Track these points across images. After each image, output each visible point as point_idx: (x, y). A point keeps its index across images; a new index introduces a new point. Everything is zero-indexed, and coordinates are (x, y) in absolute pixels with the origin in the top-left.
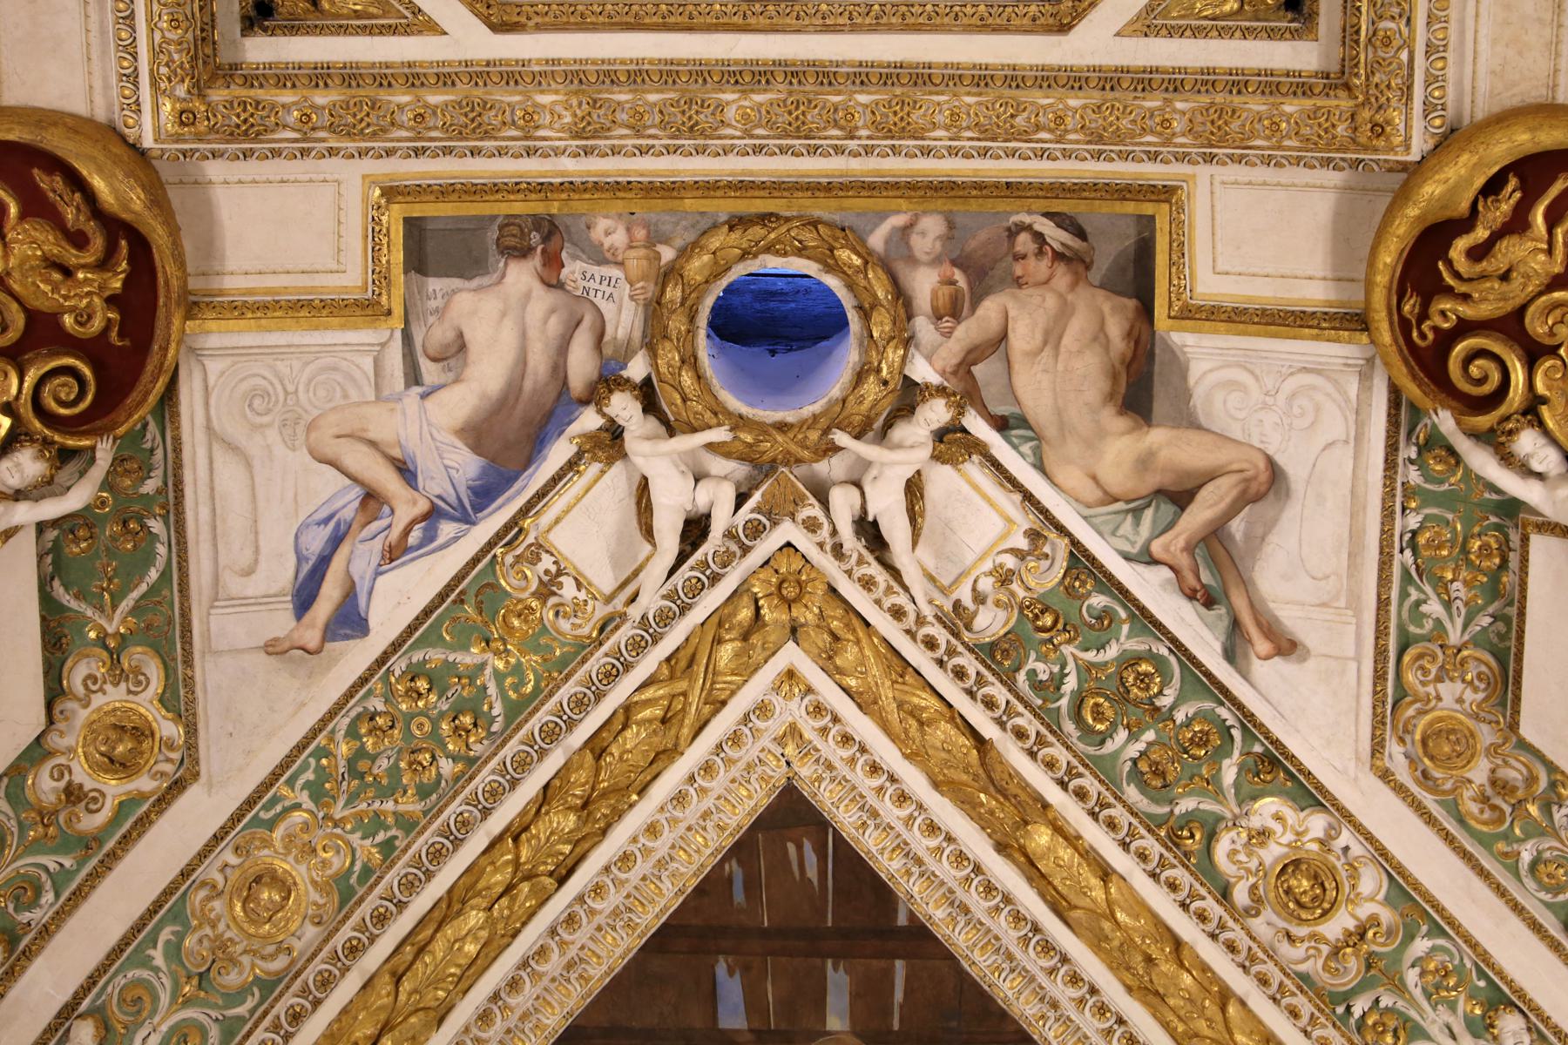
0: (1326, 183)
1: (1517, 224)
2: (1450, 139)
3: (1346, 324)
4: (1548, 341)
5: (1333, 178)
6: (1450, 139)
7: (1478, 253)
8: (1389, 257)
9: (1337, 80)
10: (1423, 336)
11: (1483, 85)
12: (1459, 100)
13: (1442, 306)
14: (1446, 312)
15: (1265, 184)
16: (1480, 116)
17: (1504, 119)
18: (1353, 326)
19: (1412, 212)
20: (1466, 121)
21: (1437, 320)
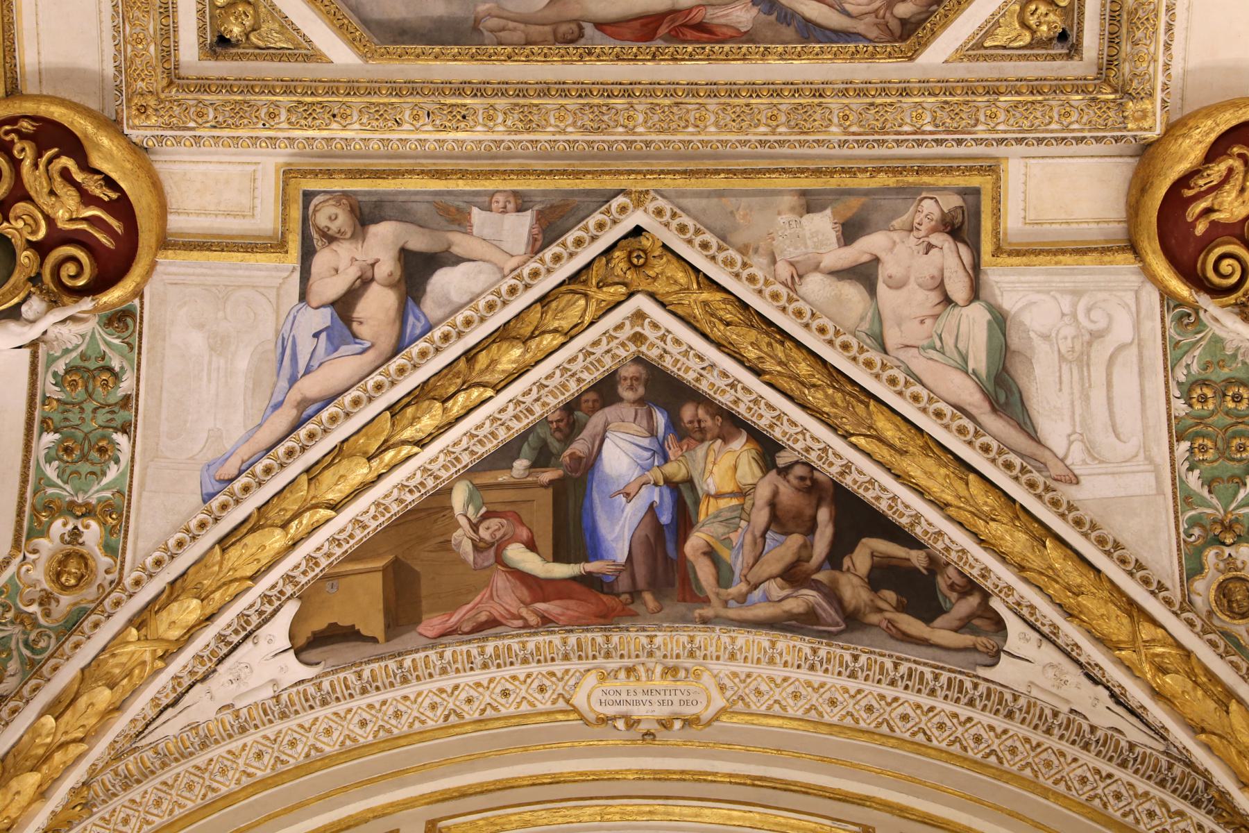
0: (105, 63)
1: (87, 199)
2: (139, 151)
3: (9, 81)
4: (11, 215)
5: (110, 70)
6: (139, 151)
7: (65, 174)
8: (57, 113)
9: (174, 77)
10: (7, 133)
11: (177, 168)
12: (165, 153)
13: (27, 149)
14: (25, 152)
15: (101, 22)
16: (157, 166)
17: (156, 186)
18: (9, 86)
19: (90, 129)
20: (153, 157)
21: (18, 146)
